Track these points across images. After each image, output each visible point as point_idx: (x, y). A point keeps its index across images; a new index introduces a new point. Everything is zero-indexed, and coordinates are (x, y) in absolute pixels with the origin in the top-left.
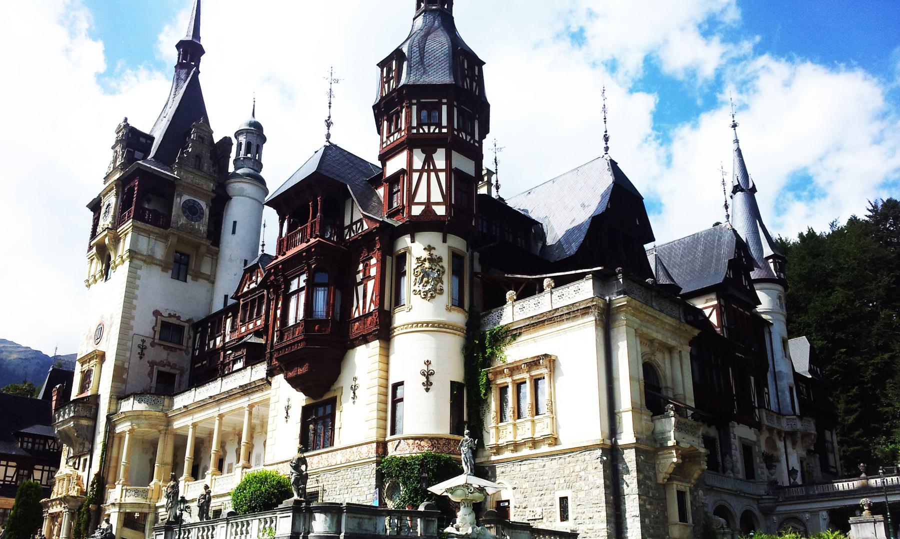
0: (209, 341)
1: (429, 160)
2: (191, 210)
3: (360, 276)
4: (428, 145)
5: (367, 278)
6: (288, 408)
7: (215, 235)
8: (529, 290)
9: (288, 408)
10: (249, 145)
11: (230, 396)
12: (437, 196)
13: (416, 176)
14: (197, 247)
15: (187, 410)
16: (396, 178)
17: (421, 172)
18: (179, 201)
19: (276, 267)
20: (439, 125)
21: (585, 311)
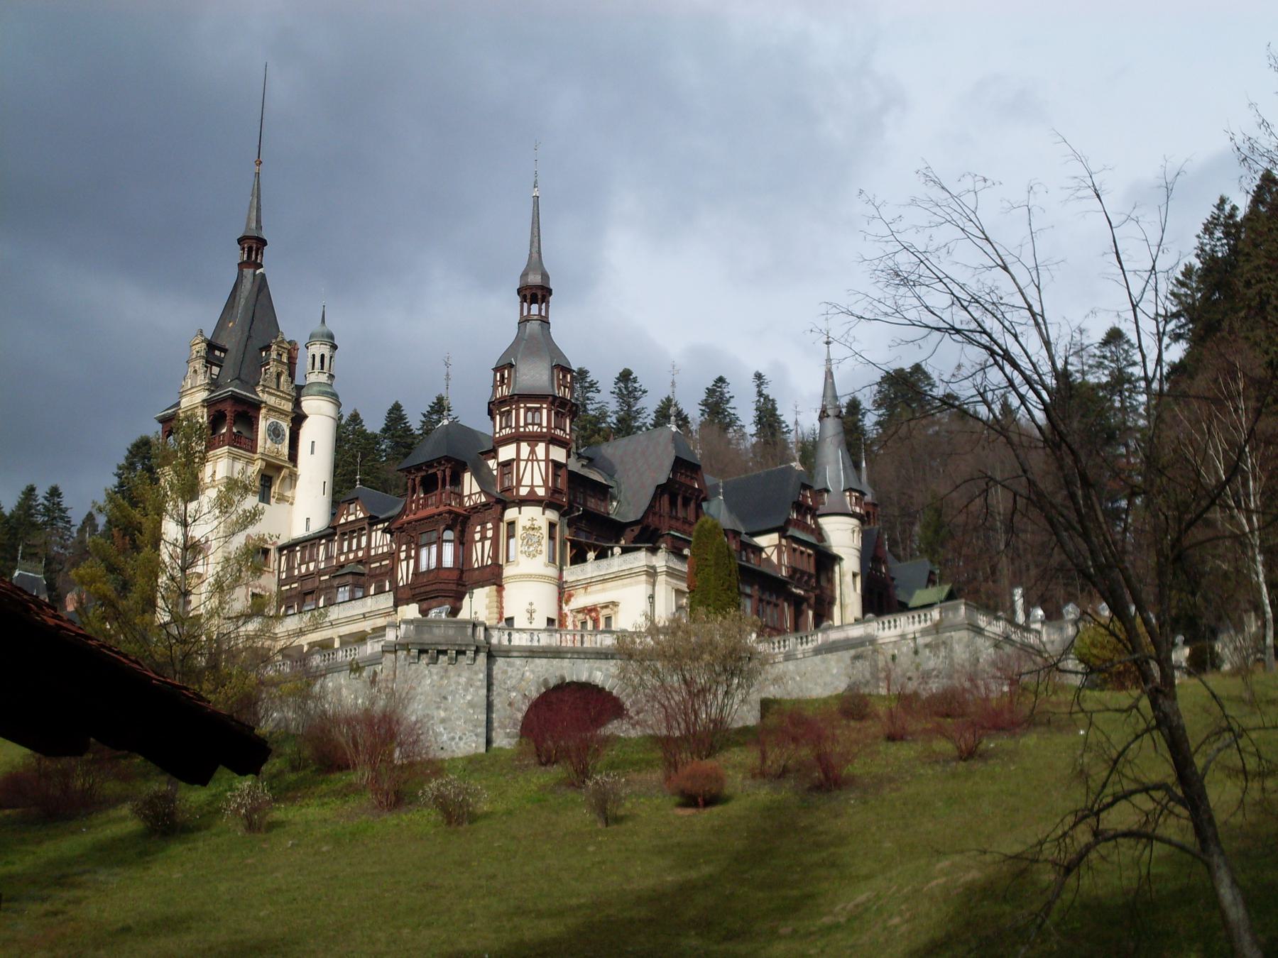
0: (299, 565)
1: (533, 452)
2: (275, 433)
3: (477, 537)
4: (533, 439)
5: (483, 538)
7: (293, 457)
8: (602, 555)
10: (323, 356)
11: (351, 620)
12: (538, 481)
13: (522, 464)
14: (279, 468)
16: (507, 464)
17: (527, 460)
18: (263, 425)
19: (409, 523)
20: (540, 425)
21: (637, 574)
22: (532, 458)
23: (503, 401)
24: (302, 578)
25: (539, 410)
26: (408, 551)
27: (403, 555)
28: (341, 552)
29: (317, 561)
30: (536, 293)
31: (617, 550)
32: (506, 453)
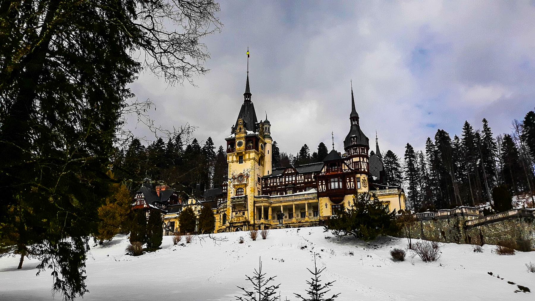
1: (363, 160)
3: (348, 181)
4: (363, 157)
5: (350, 181)
6: (326, 205)
9: (326, 205)
11: (300, 200)
12: (365, 168)
15: (281, 202)
21: (396, 194)
22: (363, 161)
23: (354, 146)
24: (271, 187)
25: (364, 149)
26: (322, 183)
27: (320, 184)
28: (285, 181)
29: (276, 182)
30: (354, 117)
31: (387, 188)
32: (356, 159)
